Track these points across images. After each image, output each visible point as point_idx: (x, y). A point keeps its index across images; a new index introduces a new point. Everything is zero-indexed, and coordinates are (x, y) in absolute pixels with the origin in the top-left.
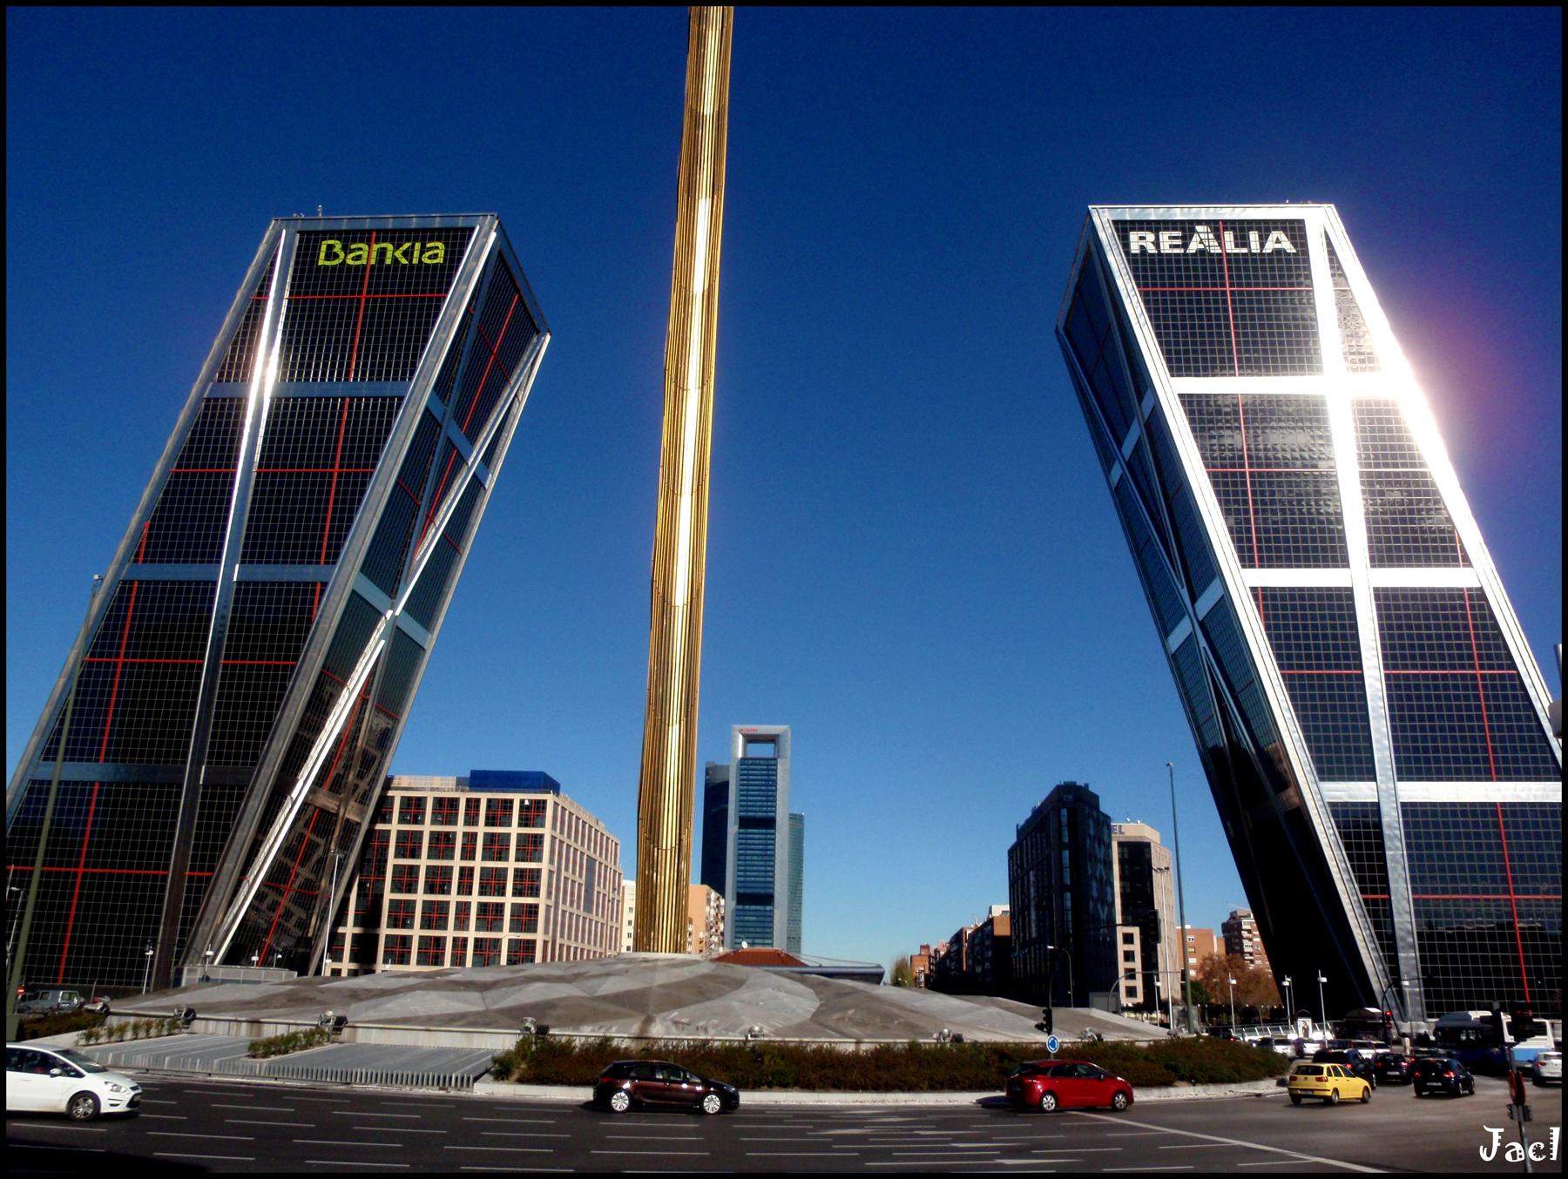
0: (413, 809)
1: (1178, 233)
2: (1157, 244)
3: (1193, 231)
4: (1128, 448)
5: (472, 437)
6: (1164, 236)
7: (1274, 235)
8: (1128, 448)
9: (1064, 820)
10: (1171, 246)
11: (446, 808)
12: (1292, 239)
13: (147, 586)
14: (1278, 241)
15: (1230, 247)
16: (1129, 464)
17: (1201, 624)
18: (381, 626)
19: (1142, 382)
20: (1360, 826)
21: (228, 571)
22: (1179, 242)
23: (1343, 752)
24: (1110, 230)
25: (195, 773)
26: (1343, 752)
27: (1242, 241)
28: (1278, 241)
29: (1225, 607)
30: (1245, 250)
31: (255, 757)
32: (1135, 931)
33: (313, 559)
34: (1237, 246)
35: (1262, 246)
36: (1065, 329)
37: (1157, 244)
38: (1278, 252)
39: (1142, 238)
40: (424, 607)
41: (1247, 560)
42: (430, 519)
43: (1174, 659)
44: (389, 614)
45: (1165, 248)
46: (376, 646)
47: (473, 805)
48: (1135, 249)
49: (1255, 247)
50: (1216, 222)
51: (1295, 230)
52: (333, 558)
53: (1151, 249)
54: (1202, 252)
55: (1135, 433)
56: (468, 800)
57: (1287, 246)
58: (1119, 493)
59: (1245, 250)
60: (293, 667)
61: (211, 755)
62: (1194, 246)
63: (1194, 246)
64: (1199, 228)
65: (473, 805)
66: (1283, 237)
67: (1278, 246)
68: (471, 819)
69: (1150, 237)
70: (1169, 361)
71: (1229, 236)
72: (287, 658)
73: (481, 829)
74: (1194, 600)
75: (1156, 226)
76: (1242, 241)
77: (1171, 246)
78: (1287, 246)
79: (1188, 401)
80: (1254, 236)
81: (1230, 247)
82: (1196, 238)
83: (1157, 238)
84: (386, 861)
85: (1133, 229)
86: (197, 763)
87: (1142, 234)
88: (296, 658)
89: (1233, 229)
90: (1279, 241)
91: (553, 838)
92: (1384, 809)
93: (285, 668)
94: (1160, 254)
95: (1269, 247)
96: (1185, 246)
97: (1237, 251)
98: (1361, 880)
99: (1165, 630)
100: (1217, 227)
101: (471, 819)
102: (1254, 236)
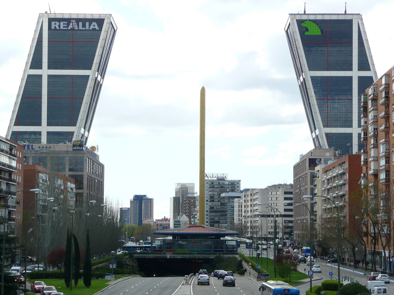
1: (66, 23)
6: (62, 23)
7: (94, 23)
10: (64, 27)
14: (94, 26)
22: (66, 25)
27: (84, 26)
28: (94, 26)
30: (84, 29)
35: (89, 28)
37: (59, 26)
38: (94, 29)
45: (62, 27)
48: (53, 27)
49: (87, 27)
53: (57, 28)
54: (73, 29)
57: (97, 27)
59: (84, 29)
62: (70, 27)
63: (70, 27)
66: (96, 24)
67: (94, 27)
69: (58, 23)
71: (81, 24)
75: (60, 20)
76: (84, 26)
77: (64, 27)
80: (87, 24)
81: (81, 27)
83: (60, 24)
90: (95, 25)
94: (60, 30)
95: (91, 27)
96: (68, 27)
97: (82, 29)
100: (78, 20)
102: (87, 24)
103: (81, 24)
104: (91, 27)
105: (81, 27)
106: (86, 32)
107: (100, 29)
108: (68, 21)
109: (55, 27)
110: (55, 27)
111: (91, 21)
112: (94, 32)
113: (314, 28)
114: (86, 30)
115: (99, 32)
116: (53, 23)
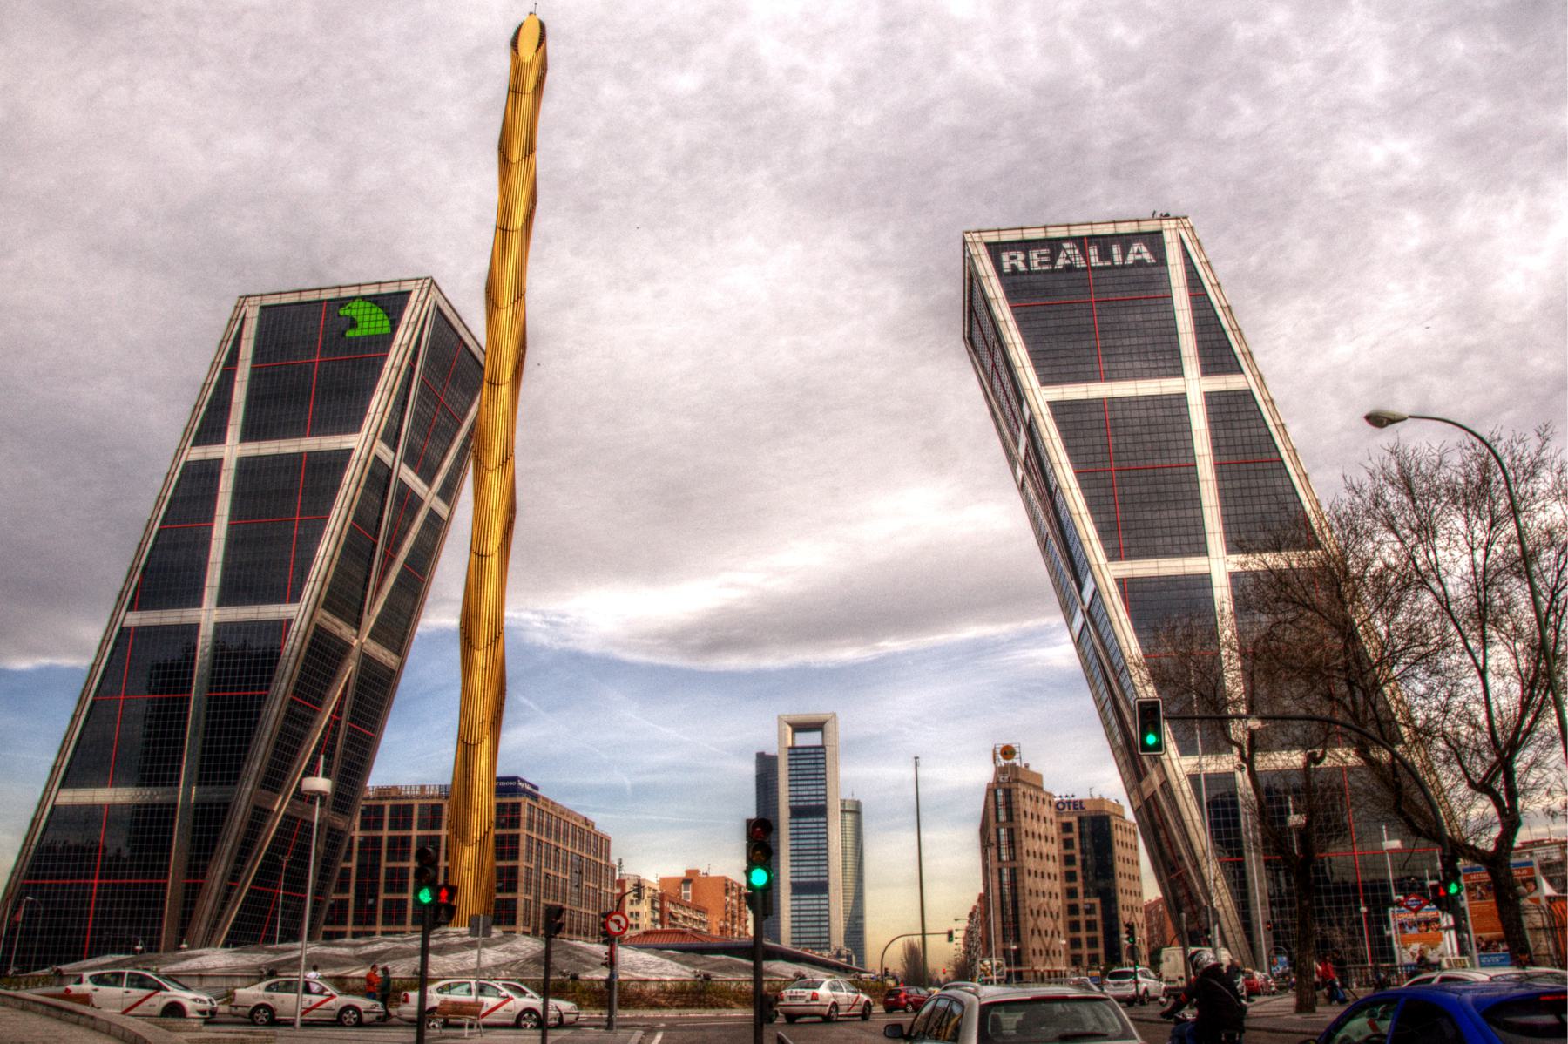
1: (1044, 251)
2: (1026, 262)
3: (1061, 248)
6: (1034, 255)
7: (1135, 248)
9: (1001, 800)
12: (1151, 252)
13: (143, 632)
14: (1139, 253)
15: (1094, 261)
19: (1019, 396)
21: (208, 615)
22: (1045, 259)
24: (983, 250)
28: (1139, 253)
31: (237, 776)
32: (1097, 901)
33: (281, 599)
34: (1101, 259)
38: (1140, 263)
39: (1013, 258)
44: (356, 642)
48: (1006, 266)
49: (1117, 259)
50: (1081, 238)
51: (1154, 240)
52: (296, 598)
53: (1021, 266)
54: (1069, 268)
57: (1147, 256)
59: (1108, 263)
61: (200, 777)
62: (1060, 263)
63: (1060, 263)
64: (1066, 245)
66: (1144, 249)
69: (1021, 256)
71: (1093, 251)
72: (260, 689)
75: (1026, 245)
76: (1105, 254)
78: (1147, 256)
79: (1057, 408)
81: (1094, 261)
82: (1062, 254)
84: (379, 866)
85: (1005, 250)
86: (188, 785)
87: (1013, 253)
88: (267, 689)
89: (1097, 243)
91: (529, 838)
93: (260, 697)
94: (1029, 272)
95: (1131, 258)
96: (1053, 262)
99: (1069, 620)
100: (1082, 243)
102: (1116, 250)
103: (1093, 251)
104: (1131, 258)
106: (1117, 273)
107: (1162, 260)
108: (1054, 245)
109: (1014, 268)
110: (1014, 268)
111: (1126, 240)
112: (1141, 271)
114: (1113, 267)
115: (1156, 270)
116: (1005, 257)
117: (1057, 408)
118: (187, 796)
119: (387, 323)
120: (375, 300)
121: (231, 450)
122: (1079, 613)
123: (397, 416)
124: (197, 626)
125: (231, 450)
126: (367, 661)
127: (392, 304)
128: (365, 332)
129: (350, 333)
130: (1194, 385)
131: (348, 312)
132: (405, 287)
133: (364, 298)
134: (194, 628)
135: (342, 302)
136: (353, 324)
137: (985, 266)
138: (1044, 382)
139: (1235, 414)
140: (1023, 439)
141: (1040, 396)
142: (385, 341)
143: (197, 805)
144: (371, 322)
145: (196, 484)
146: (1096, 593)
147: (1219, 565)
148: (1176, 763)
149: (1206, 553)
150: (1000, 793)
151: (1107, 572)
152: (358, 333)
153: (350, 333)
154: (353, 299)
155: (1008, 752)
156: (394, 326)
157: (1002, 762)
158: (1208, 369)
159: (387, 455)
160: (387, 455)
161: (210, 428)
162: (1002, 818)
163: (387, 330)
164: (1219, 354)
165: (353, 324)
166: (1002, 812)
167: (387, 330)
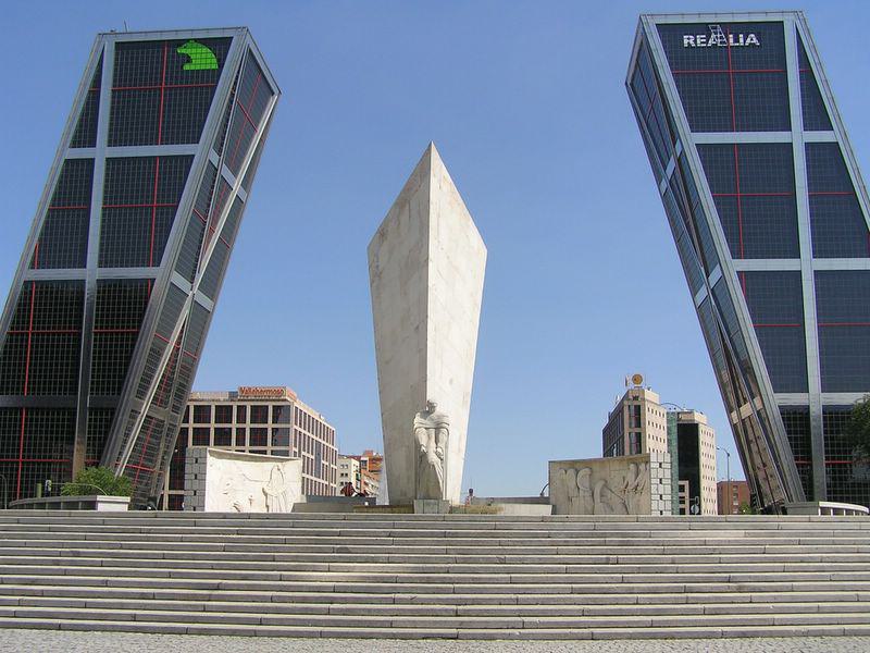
0: (202, 413)
4: (670, 171)
5: (235, 173)
8: (670, 171)
11: (224, 413)
16: (670, 182)
17: (712, 290)
18: (188, 303)
19: (674, 137)
20: (796, 420)
21: (92, 273)
23: (790, 374)
25: (83, 400)
26: (790, 374)
29: (722, 279)
31: (120, 389)
36: (632, 84)
40: (211, 286)
41: (736, 255)
42: (212, 231)
43: (699, 309)
44: (190, 294)
46: (185, 312)
47: (241, 409)
52: (157, 263)
55: (672, 165)
56: (238, 407)
58: (664, 197)
60: (138, 332)
61: (92, 389)
65: (241, 409)
68: (241, 419)
70: (690, 121)
73: (248, 425)
74: (708, 276)
79: (702, 149)
81: (731, 41)
86: (84, 394)
88: (139, 327)
92: (812, 409)
93: (133, 333)
98: (796, 452)
99: (694, 293)
101: (241, 419)
105: (731, 41)
113: (209, 61)
117: (702, 149)
118: (84, 402)
119: (215, 61)
120: (205, 42)
121: (101, 152)
122: (704, 288)
123: (221, 132)
124: (84, 281)
125: (101, 152)
126: (196, 305)
127: (220, 46)
128: (198, 68)
129: (187, 67)
130: (798, 137)
131: (183, 51)
132: (227, 34)
133: (196, 40)
134: (82, 282)
135: (180, 43)
136: (189, 60)
137: (656, 42)
138: (695, 128)
139: (828, 160)
140: (672, 165)
141: (691, 140)
142: (215, 75)
143: (91, 409)
144: (202, 59)
145: (74, 177)
146: (722, 279)
147: (807, 264)
148: (771, 398)
149: (817, 273)
150: (632, 408)
151: (733, 267)
152: (193, 68)
153: (187, 67)
154: (188, 40)
155: (637, 379)
156: (221, 66)
157: (632, 385)
158: (808, 126)
159: (214, 158)
160: (214, 158)
161: (85, 134)
162: (633, 425)
163: (215, 66)
164: (817, 116)
165: (189, 60)
166: (633, 421)
167: (215, 66)
